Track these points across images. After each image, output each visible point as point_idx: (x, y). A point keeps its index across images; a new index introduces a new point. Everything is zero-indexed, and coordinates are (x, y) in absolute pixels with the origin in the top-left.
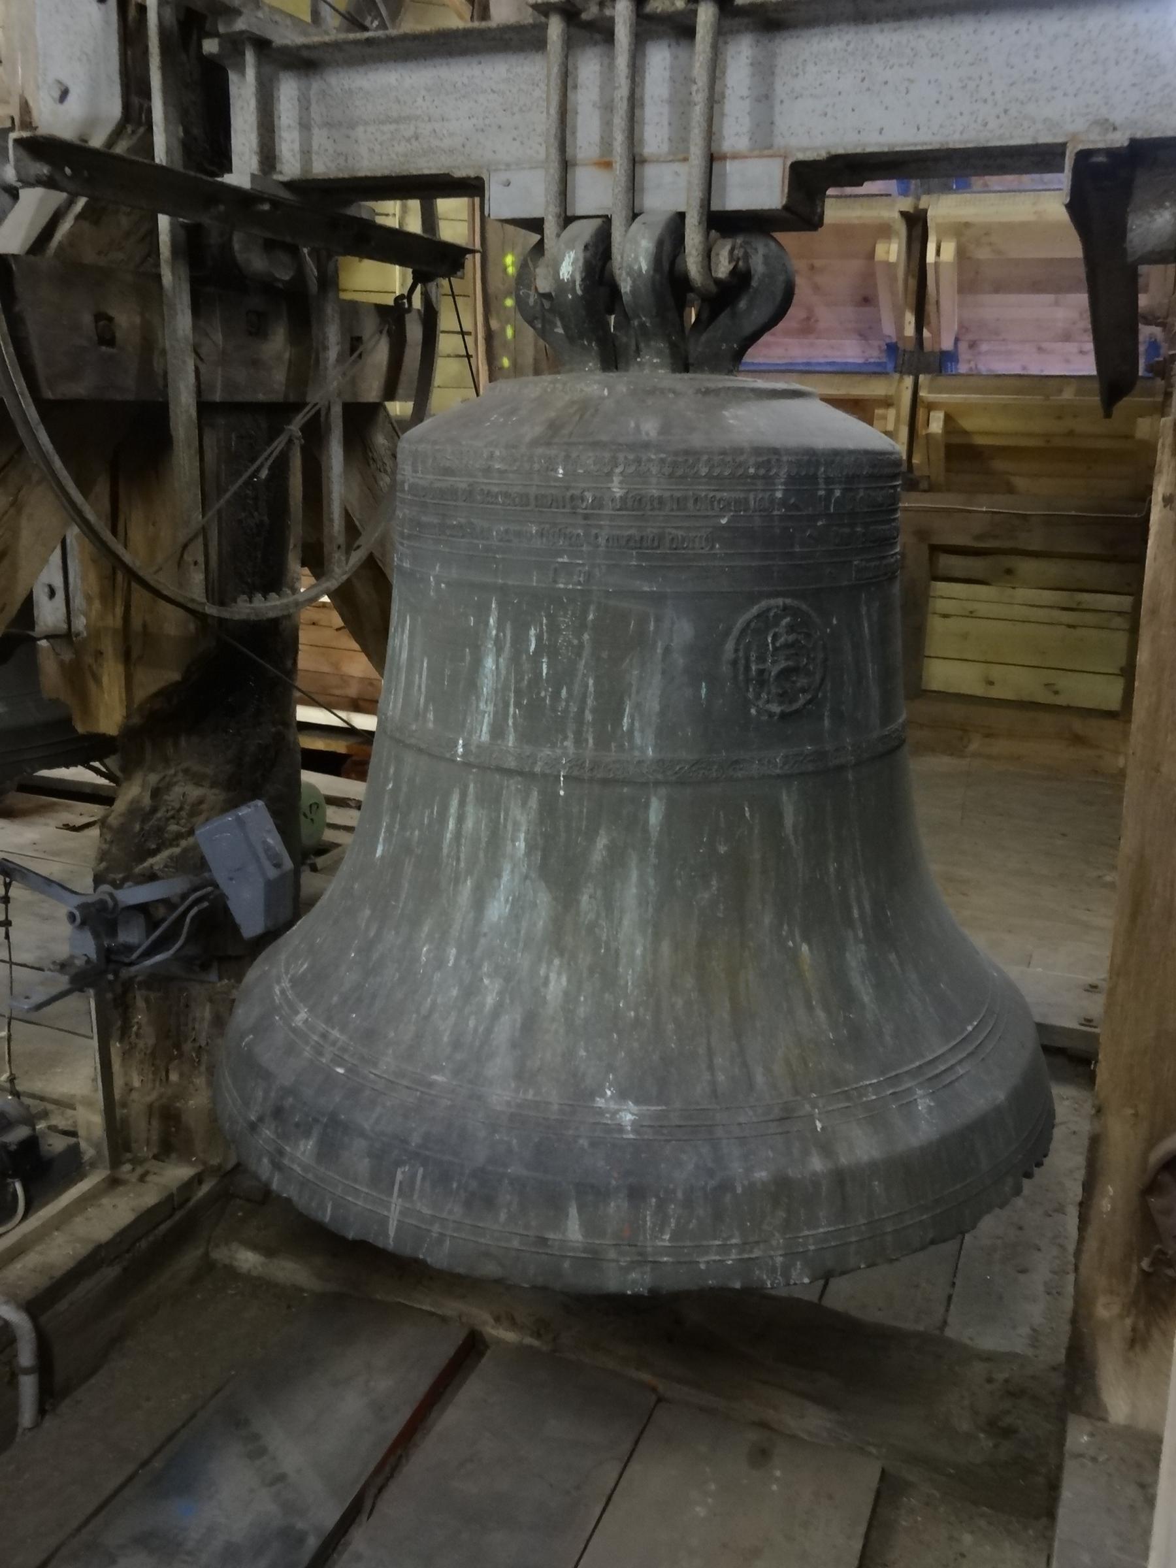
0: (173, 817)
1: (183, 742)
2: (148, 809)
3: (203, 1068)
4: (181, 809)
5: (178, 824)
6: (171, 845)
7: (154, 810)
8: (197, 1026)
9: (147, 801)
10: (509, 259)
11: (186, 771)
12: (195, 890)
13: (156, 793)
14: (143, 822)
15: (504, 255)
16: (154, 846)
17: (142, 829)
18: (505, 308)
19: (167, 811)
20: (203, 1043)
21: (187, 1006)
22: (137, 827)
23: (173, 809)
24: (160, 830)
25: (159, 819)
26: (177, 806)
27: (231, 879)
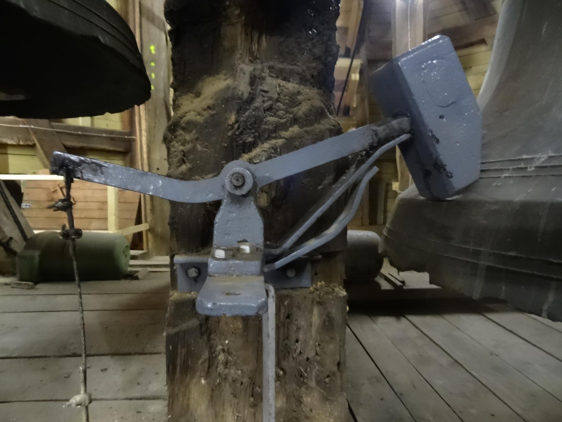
0: (270, 109)
1: (264, 44)
2: (246, 96)
3: (313, 384)
4: (277, 100)
5: (275, 115)
6: (269, 138)
7: (252, 99)
8: (301, 337)
9: (244, 88)
10: (152, 48)
11: (270, 68)
12: (381, 143)
13: (254, 80)
14: (239, 112)
15: (150, 45)
16: (250, 139)
17: (237, 121)
18: (151, 66)
19: (264, 102)
20: (311, 355)
21: (288, 317)
22: (233, 118)
23: (270, 99)
24: (258, 121)
25: (257, 109)
26: (276, 96)
27: (441, 117)
